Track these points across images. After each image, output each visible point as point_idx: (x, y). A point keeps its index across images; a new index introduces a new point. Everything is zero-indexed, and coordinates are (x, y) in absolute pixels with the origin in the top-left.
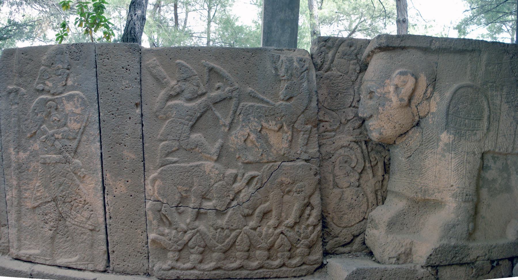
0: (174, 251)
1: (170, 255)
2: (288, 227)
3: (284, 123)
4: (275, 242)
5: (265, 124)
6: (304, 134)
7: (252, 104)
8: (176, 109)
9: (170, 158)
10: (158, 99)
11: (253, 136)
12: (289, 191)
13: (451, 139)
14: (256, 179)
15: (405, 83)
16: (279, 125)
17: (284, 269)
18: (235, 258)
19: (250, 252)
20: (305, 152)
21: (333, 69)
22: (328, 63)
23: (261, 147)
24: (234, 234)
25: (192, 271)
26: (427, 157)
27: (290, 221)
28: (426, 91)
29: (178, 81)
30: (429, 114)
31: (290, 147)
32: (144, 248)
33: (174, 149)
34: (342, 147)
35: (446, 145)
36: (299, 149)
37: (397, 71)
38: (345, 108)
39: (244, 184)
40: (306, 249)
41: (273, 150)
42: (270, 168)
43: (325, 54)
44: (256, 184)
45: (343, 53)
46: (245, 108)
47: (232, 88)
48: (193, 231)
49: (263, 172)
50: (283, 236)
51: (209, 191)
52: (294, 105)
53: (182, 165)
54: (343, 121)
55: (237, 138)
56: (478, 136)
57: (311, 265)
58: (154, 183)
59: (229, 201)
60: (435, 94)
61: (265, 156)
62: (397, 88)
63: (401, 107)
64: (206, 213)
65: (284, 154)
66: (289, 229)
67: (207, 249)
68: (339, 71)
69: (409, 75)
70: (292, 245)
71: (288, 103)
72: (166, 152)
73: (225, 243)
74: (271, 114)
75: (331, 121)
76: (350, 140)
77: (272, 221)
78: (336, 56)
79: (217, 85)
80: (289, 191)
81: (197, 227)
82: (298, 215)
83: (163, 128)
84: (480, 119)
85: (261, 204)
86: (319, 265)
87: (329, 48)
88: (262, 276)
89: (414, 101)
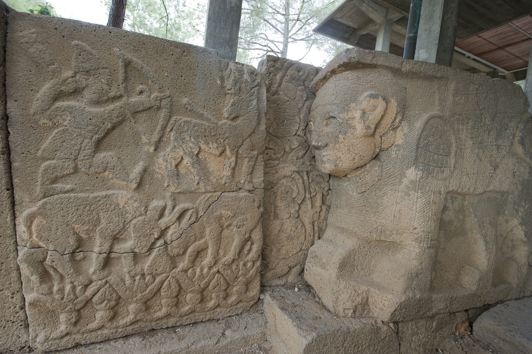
0: (71, 311)
1: (63, 317)
3: (227, 147)
4: (209, 283)
5: (203, 146)
6: (249, 161)
7: (189, 119)
9: (59, 186)
10: (39, 95)
11: (187, 160)
12: (229, 225)
13: (419, 176)
14: (190, 213)
15: (375, 107)
16: (221, 149)
17: (218, 310)
19: (179, 297)
22: (276, 85)
24: (158, 279)
25: (99, 332)
26: (385, 194)
28: (395, 119)
29: (76, 73)
30: (393, 147)
31: (233, 174)
34: (285, 177)
35: (412, 182)
36: (242, 178)
37: (366, 94)
38: (290, 136)
39: (175, 219)
41: (212, 178)
42: (208, 199)
44: (190, 219)
45: (291, 77)
48: (99, 282)
51: (124, 228)
52: (241, 126)
53: (81, 195)
54: (287, 149)
55: (167, 161)
58: (32, 222)
59: (153, 241)
60: (403, 124)
61: (202, 184)
62: (364, 113)
63: (367, 136)
64: (119, 258)
67: (121, 301)
68: (286, 95)
69: (380, 98)
74: (212, 134)
75: (276, 149)
76: (293, 170)
77: (208, 259)
78: (284, 80)
79: (139, 88)
80: (229, 225)
81: (107, 277)
83: (48, 141)
84: (448, 155)
85: (195, 241)
86: (255, 301)
87: (278, 70)
89: (380, 131)
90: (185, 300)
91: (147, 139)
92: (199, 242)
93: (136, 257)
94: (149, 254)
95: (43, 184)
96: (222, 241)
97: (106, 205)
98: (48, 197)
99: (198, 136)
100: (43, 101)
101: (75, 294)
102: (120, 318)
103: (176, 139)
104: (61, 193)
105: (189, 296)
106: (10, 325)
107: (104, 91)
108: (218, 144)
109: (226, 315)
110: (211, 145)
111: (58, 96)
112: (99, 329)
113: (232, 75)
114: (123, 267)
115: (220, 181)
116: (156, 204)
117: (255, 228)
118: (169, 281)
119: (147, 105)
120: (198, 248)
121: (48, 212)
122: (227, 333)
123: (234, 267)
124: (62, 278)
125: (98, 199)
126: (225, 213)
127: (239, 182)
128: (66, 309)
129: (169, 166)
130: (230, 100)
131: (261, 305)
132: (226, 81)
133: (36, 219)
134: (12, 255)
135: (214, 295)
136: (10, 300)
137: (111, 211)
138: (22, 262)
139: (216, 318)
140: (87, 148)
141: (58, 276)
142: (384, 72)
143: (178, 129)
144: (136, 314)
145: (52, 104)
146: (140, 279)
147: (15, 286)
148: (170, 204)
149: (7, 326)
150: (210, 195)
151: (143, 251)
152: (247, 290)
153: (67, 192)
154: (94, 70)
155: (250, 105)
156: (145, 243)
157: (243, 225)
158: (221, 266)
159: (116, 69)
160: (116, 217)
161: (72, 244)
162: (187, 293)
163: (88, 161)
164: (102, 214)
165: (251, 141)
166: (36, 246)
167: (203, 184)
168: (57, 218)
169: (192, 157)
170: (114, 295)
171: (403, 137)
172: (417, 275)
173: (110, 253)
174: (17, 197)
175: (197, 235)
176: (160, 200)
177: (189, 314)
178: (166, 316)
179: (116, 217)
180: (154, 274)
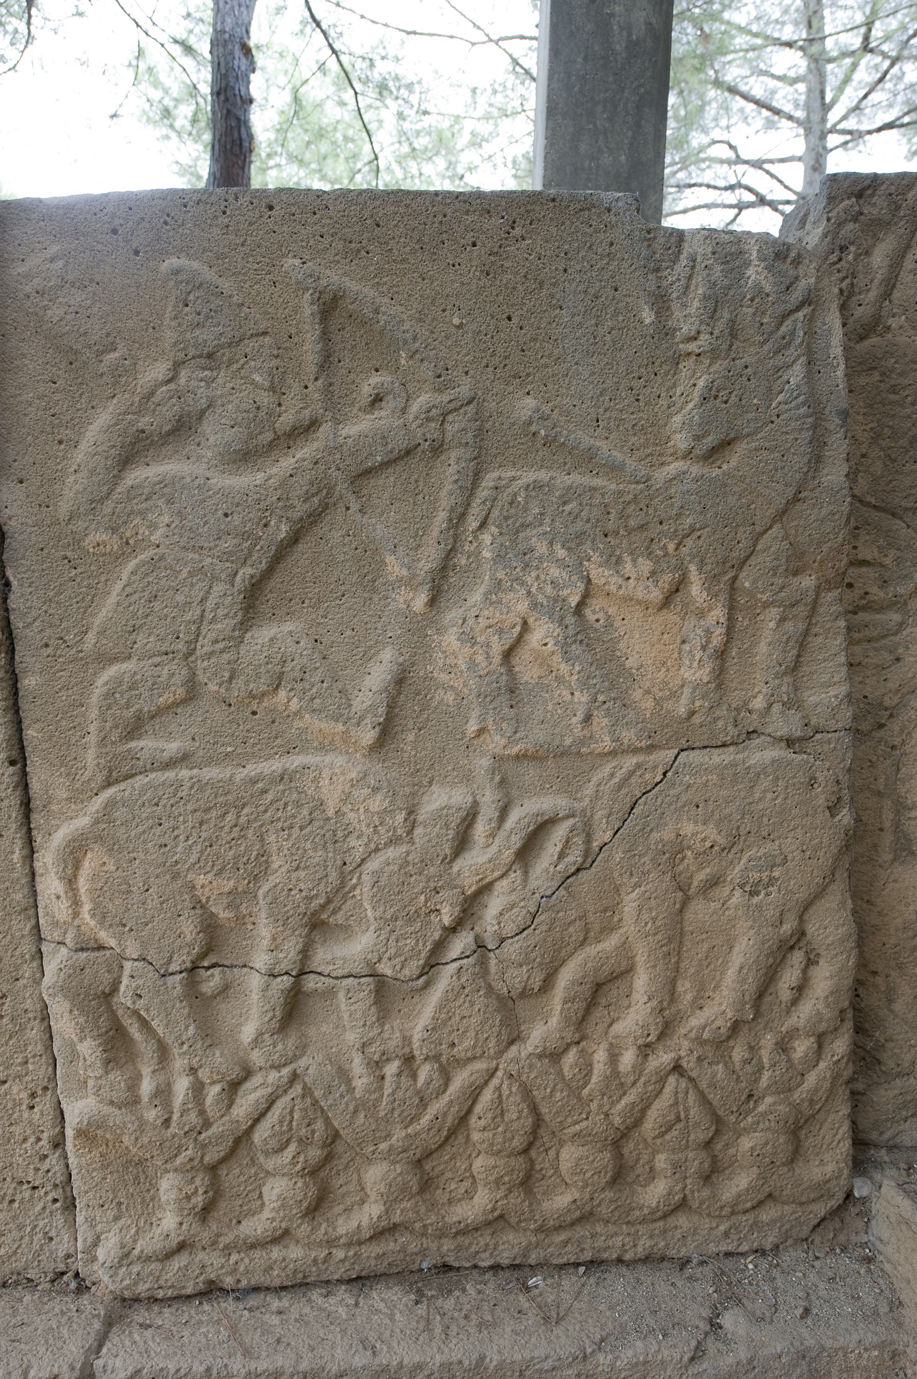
0: (189, 1169)
1: (168, 1186)
3: (693, 568)
5: (599, 574)
6: (782, 620)
7: (543, 475)
8: (170, 502)
9: (147, 745)
10: (80, 455)
11: (543, 633)
12: (714, 882)
14: (559, 833)
16: (666, 580)
17: (682, 1221)
18: (467, 1184)
19: (533, 1153)
21: (893, 323)
22: (872, 295)
23: (584, 684)
24: (460, 1080)
25: (276, 1253)
29: (177, 366)
31: (720, 675)
32: (46, 1166)
33: (166, 698)
39: (508, 855)
41: (637, 694)
43: (857, 256)
44: (562, 855)
46: (505, 497)
47: (446, 398)
48: (273, 1076)
49: (597, 796)
50: (683, 1084)
51: (342, 891)
52: (742, 479)
55: (473, 641)
58: (77, 866)
59: (437, 935)
61: (601, 722)
64: (331, 993)
65: (692, 713)
66: (709, 1051)
67: (340, 1148)
70: (718, 1121)
71: (717, 471)
72: (129, 714)
73: (425, 1120)
74: (632, 523)
75: (887, 561)
77: (635, 1015)
80: (714, 882)
81: (295, 1058)
83: (112, 599)
85: (583, 943)
86: (833, 1203)
87: (876, 228)
90: (557, 1170)
91: (403, 565)
92: (599, 947)
93: (383, 993)
94: (427, 985)
95: (102, 742)
96: (688, 944)
97: (286, 804)
98: (117, 781)
99: (580, 536)
100: (92, 472)
101: (202, 1112)
102: (338, 1209)
103: (500, 557)
104: (153, 770)
105: (569, 1155)
106: (27, 1194)
107: (262, 414)
108: (657, 561)
109: (713, 1248)
111: (133, 449)
112: (276, 1240)
113: (698, 278)
114: (344, 1025)
115: (668, 705)
116: (444, 799)
117: (819, 894)
118: (498, 1088)
119: (399, 443)
120: (596, 970)
121: (121, 833)
122: (728, 1320)
124: (163, 1052)
125: (260, 785)
127: (745, 706)
128: (178, 1161)
129: (480, 658)
131: (860, 1224)
132: (675, 306)
133: (89, 855)
134: (27, 971)
135: (661, 1161)
136: (26, 1115)
137: (302, 828)
138: (55, 995)
139: (672, 1253)
140: (221, 612)
141: (152, 1045)
143: (507, 518)
144: (390, 1202)
145: (118, 478)
146: (399, 1075)
147: (39, 1071)
148: (489, 800)
149: (18, 1197)
150: (631, 761)
151: (406, 972)
152: (796, 1154)
153: (170, 764)
154: (230, 345)
155: (776, 389)
156: (410, 942)
157: (772, 881)
158: (686, 1044)
159: (293, 331)
160: (315, 849)
161: (189, 938)
162: (562, 1143)
163: (226, 656)
164: (272, 838)
165: (786, 537)
166: (92, 944)
167: (605, 721)
168: (146, 852)
169: (562, 618)
170: (319, 1125)
173: (302, 973)
174: (35, 786)
175: (591, 918)
176: (453, 785)
177: (573, 1224)
178: (489, 1223)
179: (315, 849)
180: (444, 1059)
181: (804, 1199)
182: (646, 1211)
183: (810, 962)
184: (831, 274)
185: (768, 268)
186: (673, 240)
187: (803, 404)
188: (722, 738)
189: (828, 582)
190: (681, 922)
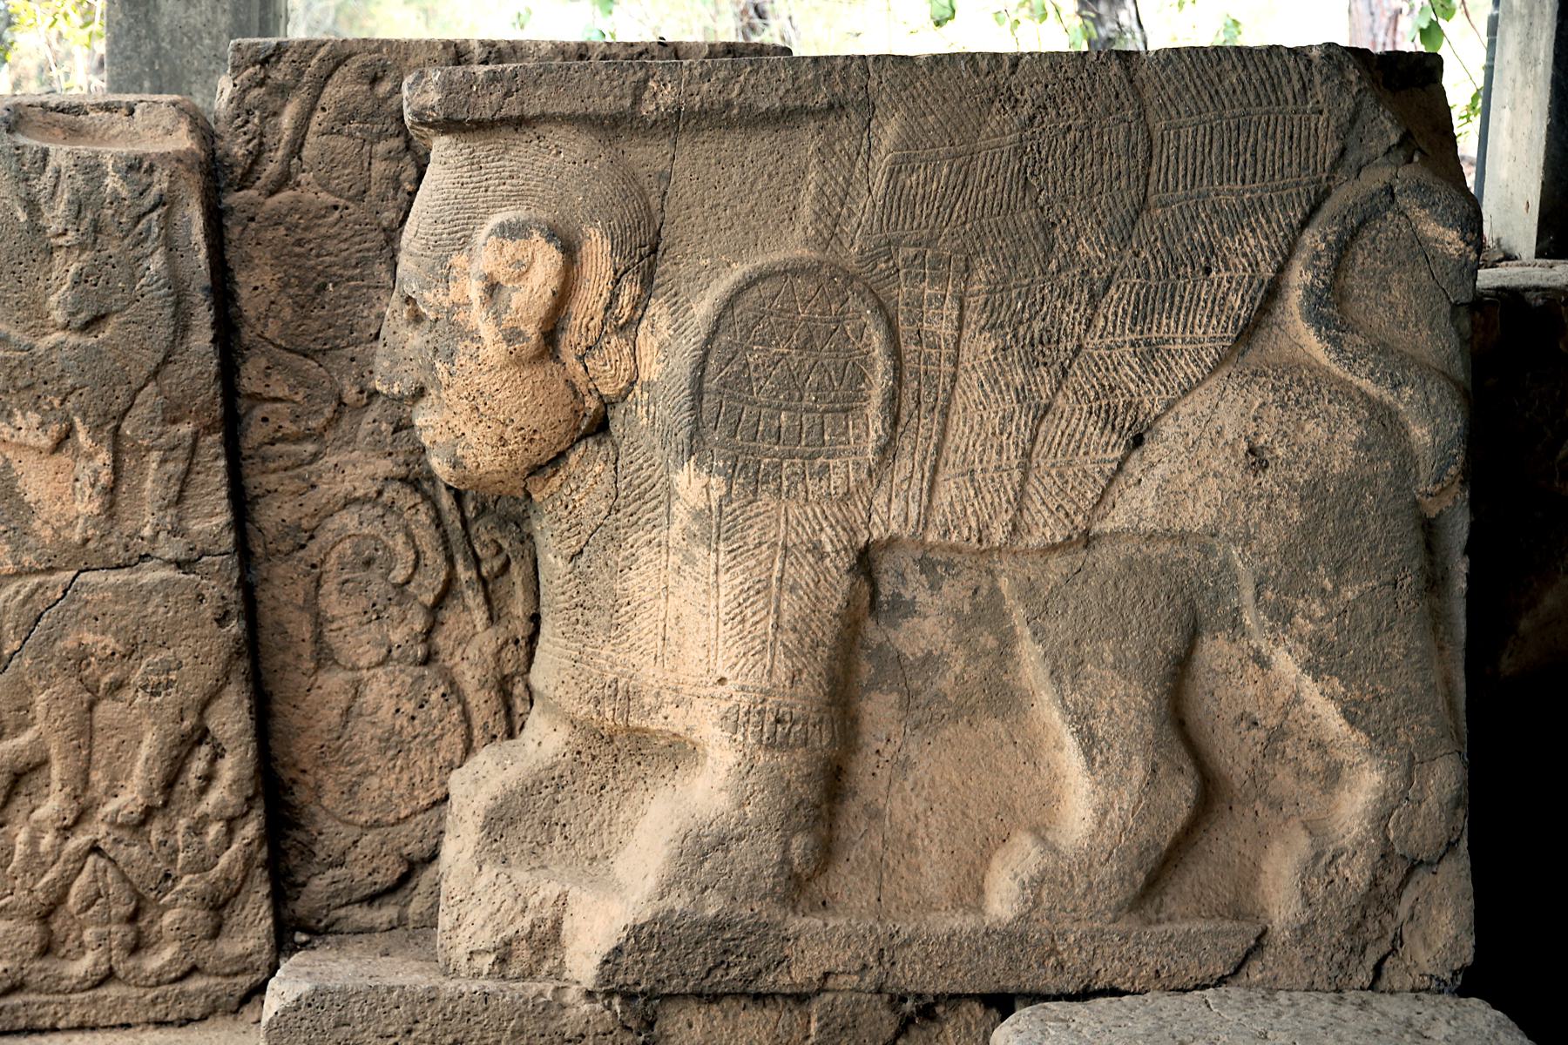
2: (122, 826)
3: (77, 420)
4: (67, 888)
6: (163, 461)
12: (117, 686)
13: (715, 495)
15: (522, 269)
16: (55, 429)
17: (112, 991)
20: (174, 532)
21: (302, 177)
27: (130, 798)
28: (615, 296)
30: (637, 389)
34: (349, 502)
35: (697, 515)
36: (145, 517)
37: (495, 220)
38: (356, 343)
40: (201, 914)
41: (37, 524)
43: (262, 120)
45: (340, 109)
50: (102, 863)
52: (116, 347)
54: (351, 394)
56: (836, 480)
57: (227, 976)
60: (654, 308)
62: (492, 288)
63: (518, 361)
65: (86, 541)
66: (125, 835)
68: (325, 187)
69: (536, 236)
71: (91, 341)
74: (20, 383)
75: (298, 398)
76: (381, 473)
77: (52, 805)
78: (314, 127)
80: (117, 686)
82: (157, 776)
84: (849, 406)
87: (283, 91)
88: (22, 1023)
89: (571, 340)
92: (16, 741)
96: (98, 740)
110: (19, 418)
113: (64, 184)
120: (12, 762)
123: (155, 834)
126: (100, 642)
127: (136, 533)
130: (66, 267)
135: (88, 935)
142: (557, 135)
155: (138, 274)
157: (169, 684)
158: (103, 829)
171: (660, 354)
172: (722, 842)
181: (227, 970)
182: (74, 981)
183: (217, 756)
184: (237, 137)
185: (124, 178)
186: (39, 155)
187: (164, 286)
188: (115, 561)
189: (206, 427)
190: (91, 719)
